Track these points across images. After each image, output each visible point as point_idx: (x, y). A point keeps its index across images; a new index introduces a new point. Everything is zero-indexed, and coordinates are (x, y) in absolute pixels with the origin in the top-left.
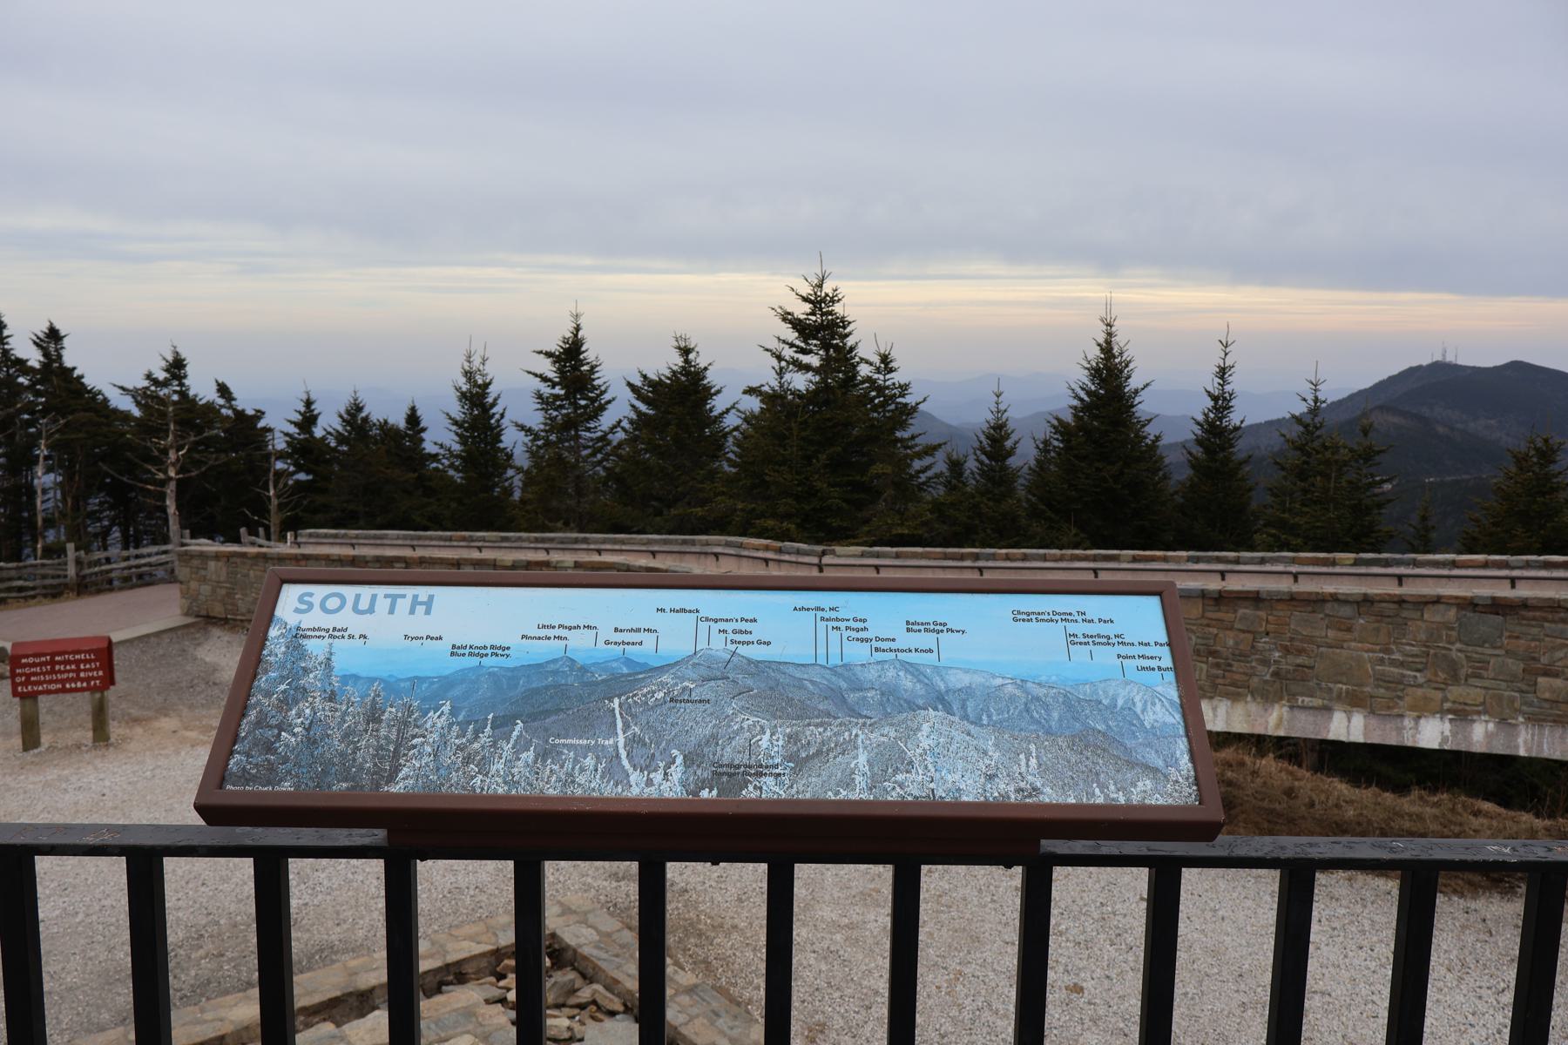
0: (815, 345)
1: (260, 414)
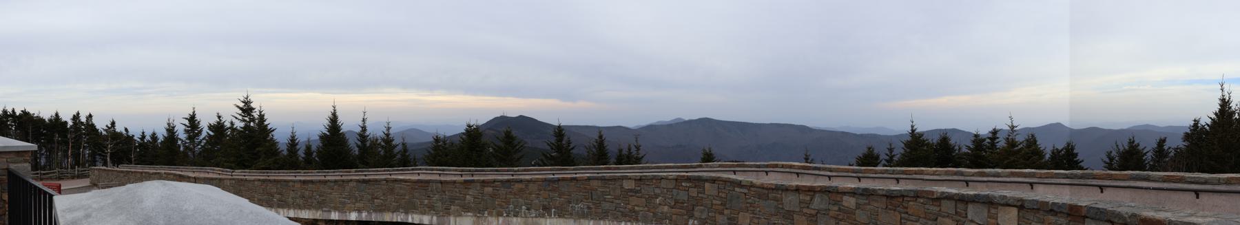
1: (133, 136)
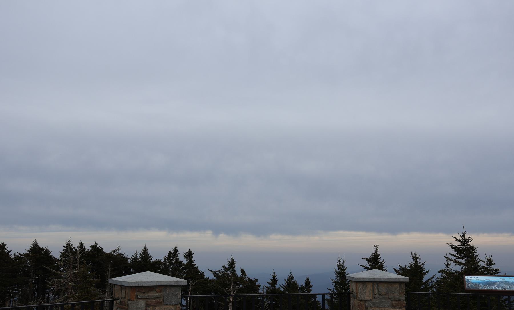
0: (463, 256)
1: (256, 280)
